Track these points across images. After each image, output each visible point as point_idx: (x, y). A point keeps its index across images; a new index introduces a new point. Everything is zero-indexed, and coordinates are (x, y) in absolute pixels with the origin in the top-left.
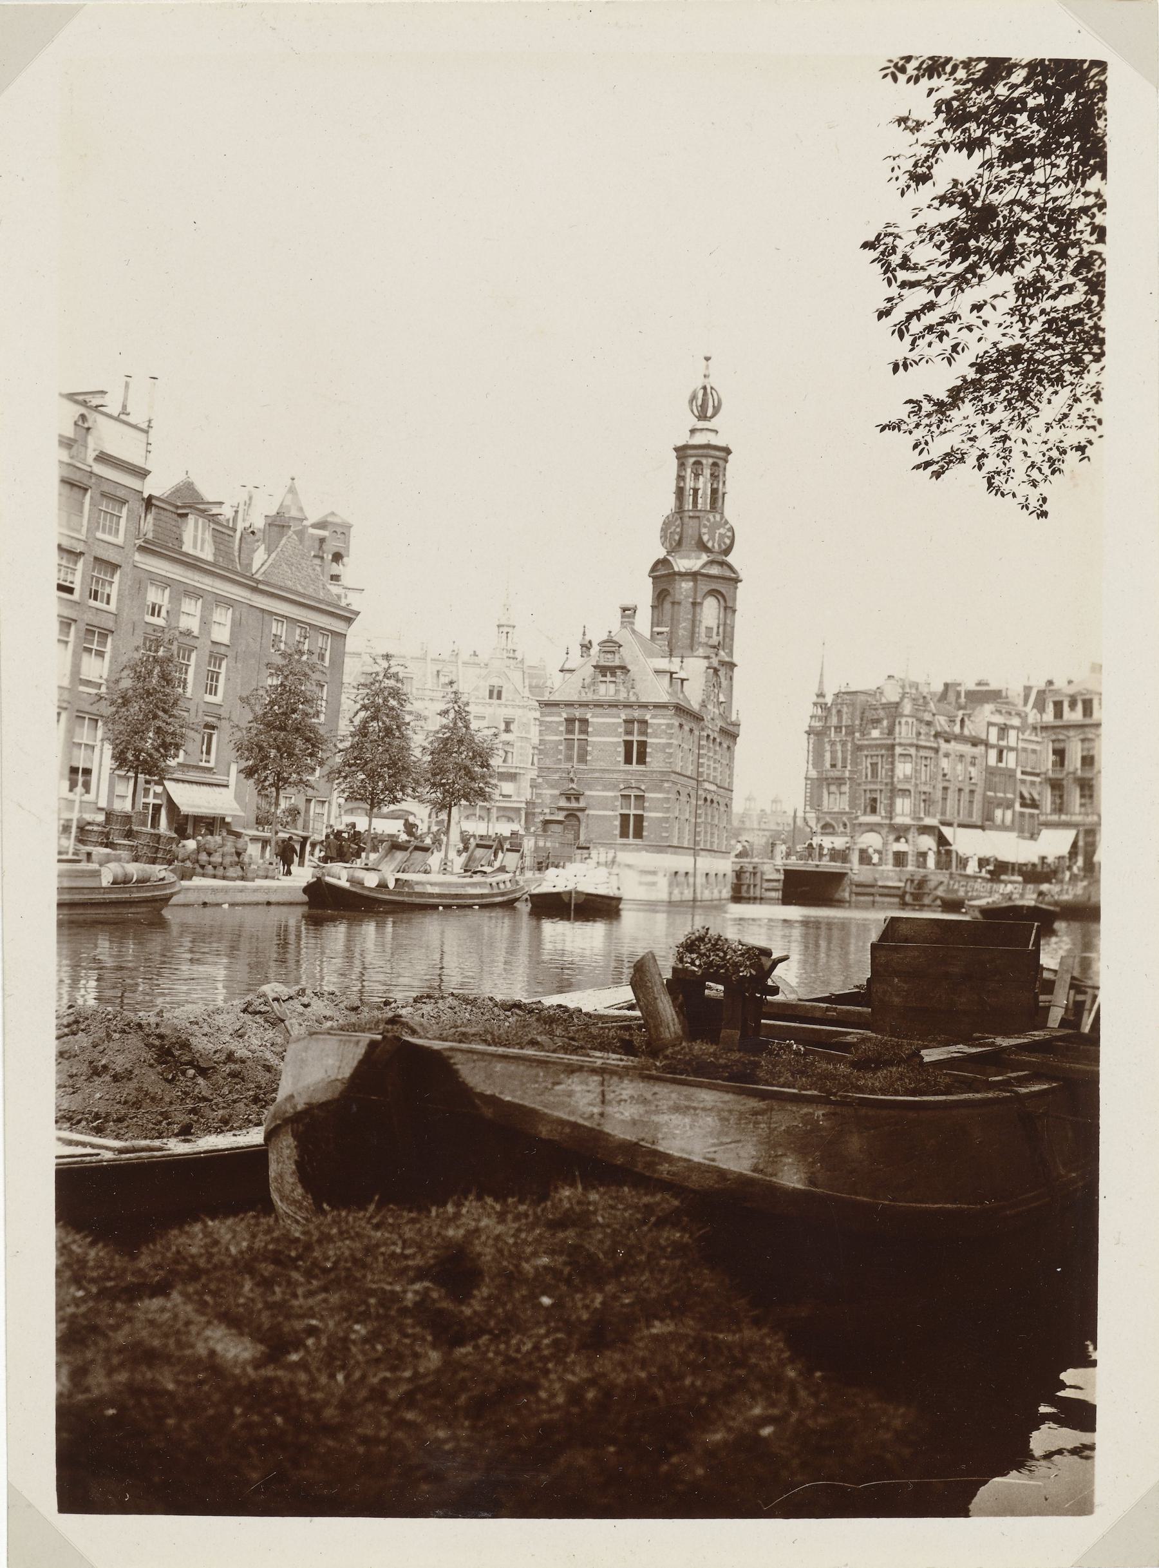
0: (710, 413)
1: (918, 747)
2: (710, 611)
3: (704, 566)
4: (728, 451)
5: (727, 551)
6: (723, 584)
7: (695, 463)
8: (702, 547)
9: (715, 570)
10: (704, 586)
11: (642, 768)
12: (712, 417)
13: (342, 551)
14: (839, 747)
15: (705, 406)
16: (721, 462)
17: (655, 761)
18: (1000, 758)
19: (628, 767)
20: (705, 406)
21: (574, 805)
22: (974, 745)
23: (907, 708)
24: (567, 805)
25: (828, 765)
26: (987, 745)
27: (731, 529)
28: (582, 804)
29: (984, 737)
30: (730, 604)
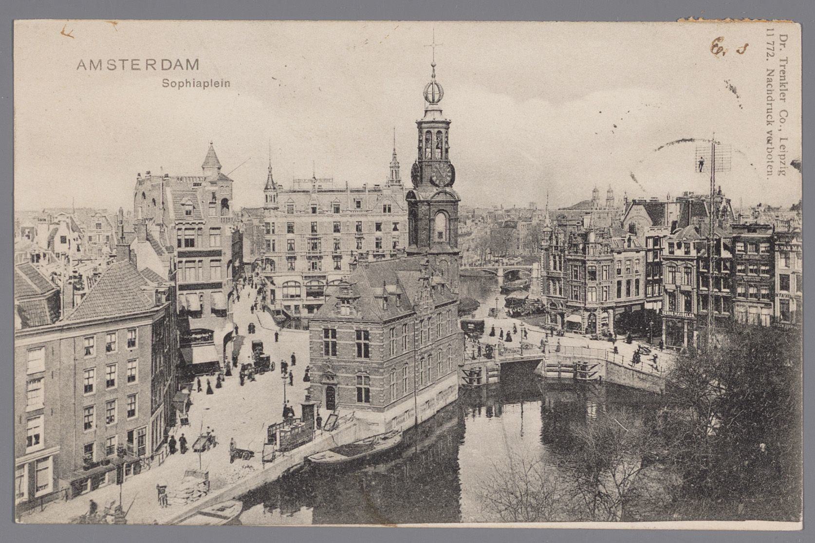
1: (599, 262)
7: (427, 132)
11: (367, 360)
12: (439, 100)
13: (228, 197)
14: (557, 258)
15: (433, 99)
16: (443, 131)
17: (375, 354)
19: (359, 359)
20: (433, 99)
21: (332, 382)
22: (638, 252)
24: (328, 381)
25: (552, 268)
28: (335, 381)
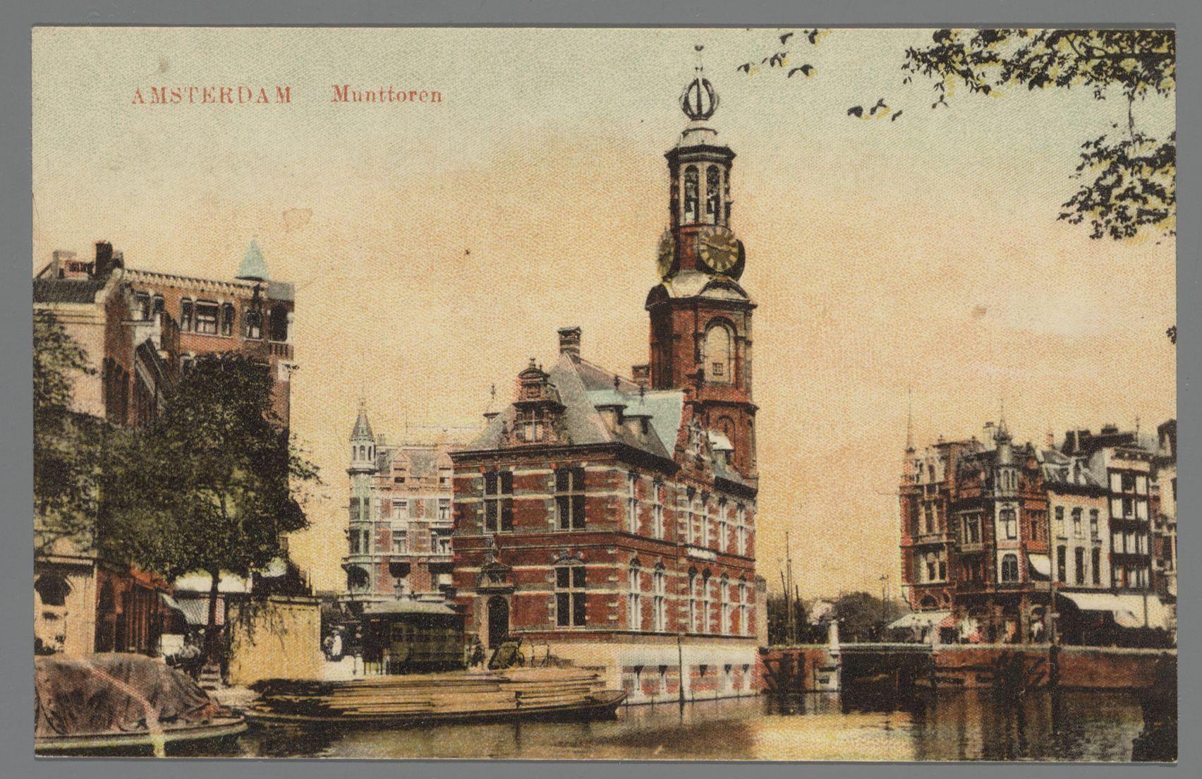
0: (705, 110)
2: (716, 343)
3: (705, 289)
4: (727, 156)
5: (737, 270)
6: (734, 314)
7: (688, 170)
8: (702, 267)
9: (719, 294)
10: (706, 316)
16: (722, 168)
18: (1127, 508)
23: (1006, 457)
26: (1111, 495)
27: (740, 245)
29: (1104, 485)
30: (741, 333)
